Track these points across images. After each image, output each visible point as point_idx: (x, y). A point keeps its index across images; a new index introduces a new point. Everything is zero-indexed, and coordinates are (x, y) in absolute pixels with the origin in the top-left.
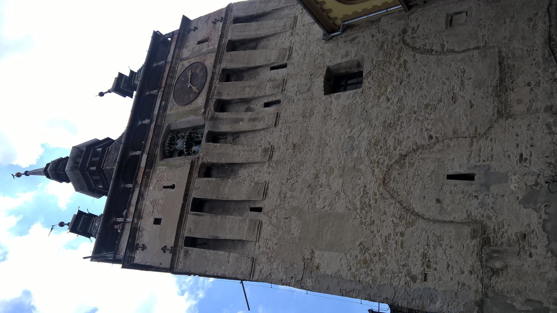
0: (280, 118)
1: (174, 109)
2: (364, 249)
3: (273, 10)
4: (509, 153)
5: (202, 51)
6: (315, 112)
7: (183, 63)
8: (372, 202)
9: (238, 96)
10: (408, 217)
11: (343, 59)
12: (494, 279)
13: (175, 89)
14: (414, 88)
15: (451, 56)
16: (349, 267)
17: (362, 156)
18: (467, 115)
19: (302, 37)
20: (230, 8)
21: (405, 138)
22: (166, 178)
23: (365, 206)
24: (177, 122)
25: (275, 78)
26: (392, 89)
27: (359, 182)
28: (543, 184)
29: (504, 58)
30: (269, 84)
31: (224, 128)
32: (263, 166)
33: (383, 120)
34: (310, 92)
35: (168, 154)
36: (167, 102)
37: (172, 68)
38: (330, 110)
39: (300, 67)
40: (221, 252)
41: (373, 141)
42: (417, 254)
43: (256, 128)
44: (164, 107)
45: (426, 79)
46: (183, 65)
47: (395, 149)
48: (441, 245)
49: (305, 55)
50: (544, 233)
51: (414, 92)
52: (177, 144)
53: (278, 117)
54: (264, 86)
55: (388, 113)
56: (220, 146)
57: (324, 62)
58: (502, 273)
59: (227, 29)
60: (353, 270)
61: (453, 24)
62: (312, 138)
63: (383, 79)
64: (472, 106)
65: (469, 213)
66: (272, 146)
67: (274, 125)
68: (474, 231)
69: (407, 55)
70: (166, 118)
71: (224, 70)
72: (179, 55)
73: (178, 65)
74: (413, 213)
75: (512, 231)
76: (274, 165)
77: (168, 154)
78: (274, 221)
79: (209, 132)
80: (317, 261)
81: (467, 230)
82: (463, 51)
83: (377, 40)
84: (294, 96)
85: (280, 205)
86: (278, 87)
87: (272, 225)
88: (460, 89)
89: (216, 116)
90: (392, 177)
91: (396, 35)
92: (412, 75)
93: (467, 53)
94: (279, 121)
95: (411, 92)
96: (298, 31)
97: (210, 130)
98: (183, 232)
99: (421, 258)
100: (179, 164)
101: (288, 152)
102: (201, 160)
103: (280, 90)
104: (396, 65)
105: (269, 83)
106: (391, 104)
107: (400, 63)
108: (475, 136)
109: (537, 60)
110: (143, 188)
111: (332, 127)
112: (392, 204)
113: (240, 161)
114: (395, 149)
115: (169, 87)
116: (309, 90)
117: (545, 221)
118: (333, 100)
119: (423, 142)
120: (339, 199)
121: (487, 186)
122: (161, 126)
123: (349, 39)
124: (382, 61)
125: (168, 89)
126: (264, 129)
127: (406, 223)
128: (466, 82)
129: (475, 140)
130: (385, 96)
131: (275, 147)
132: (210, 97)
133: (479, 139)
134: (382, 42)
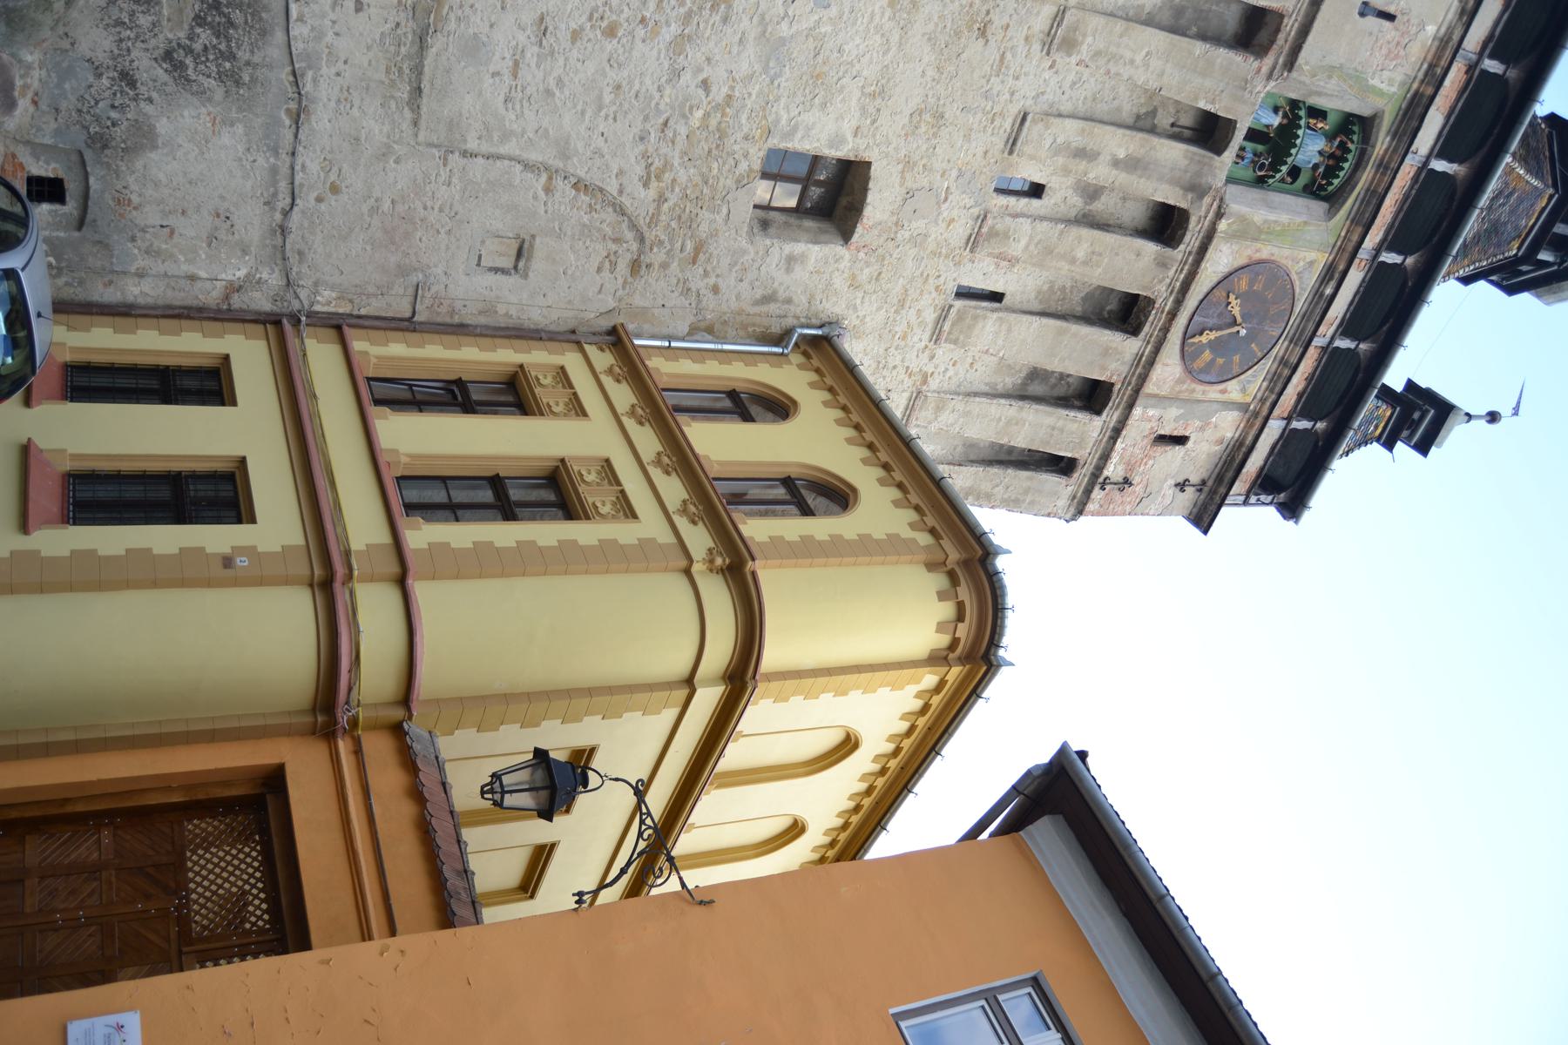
0: (1007, 134)
1: (1302, 264)
3: (960, 465)
5: (1182, 411)
6: (906, 120)
7: (1241, 395)
9: (1113, 240)
11: (803, 252)
13: (1284, 325)
14: (637, 96)
15: (533, 156)
19: (899, 358)
22: (1379, 44)
24: (1303, 218)
25: (997, 266)
30: (1016, 249)
31: (1175, 154)
34: (909, 184)
35: (1356, 128)
36: (1317, 293)
37: (1277, 389)
38: (863, 109)
39: (922, 275)
43: (1081, 126)
44: (1331, 279)
45: (603, 113)
46: (1244, 390)
49: (902, 303)
51: (637, 87)
52: (1320, 153)
53: (1011, 141)
54: (1032, 247)
55: (712, 44)
56: (1196, 99)
57: (854, 261)
59: (1096, 450)
61: (515, 246)
62: (929, 39)
63: (710, 152)
66: (1048, 53)
67: (1029, 118)
69: (640, 199)
70: (1332, 241)
71: (1134, 331)
72: (1249, 424)
77: (1356, 128)
79: (1219, 152)
82: (499, 157)
83: (706, 274)
84: (953, 189)
86: (993, 234)
88: (523, 51)
89: (1190, 196)
91: (656, 268)
92: (634, 138)
93: (493, 150)
95: (644, 90)
96: (908, 382)
97: (1216, 157)
100: (1330, 77)
101: (1006, 20)
102: (1265, 70)
103: (990, 222)
104: (670, 181)
105: (1014, 253)
109: (333, 71)
110: (1456, 37)
111: (868, 56)
113: (1150, 32)
115: (1301, 334)
116: (910, 194)
118: (850, 138)
122: (1352, 221)
123: (779, 305)
124: (704, 208)
126: (1060, 115)
130: (713, 100)
131: (1039, 48)
132: (1191, 258)
134: (694, 262)
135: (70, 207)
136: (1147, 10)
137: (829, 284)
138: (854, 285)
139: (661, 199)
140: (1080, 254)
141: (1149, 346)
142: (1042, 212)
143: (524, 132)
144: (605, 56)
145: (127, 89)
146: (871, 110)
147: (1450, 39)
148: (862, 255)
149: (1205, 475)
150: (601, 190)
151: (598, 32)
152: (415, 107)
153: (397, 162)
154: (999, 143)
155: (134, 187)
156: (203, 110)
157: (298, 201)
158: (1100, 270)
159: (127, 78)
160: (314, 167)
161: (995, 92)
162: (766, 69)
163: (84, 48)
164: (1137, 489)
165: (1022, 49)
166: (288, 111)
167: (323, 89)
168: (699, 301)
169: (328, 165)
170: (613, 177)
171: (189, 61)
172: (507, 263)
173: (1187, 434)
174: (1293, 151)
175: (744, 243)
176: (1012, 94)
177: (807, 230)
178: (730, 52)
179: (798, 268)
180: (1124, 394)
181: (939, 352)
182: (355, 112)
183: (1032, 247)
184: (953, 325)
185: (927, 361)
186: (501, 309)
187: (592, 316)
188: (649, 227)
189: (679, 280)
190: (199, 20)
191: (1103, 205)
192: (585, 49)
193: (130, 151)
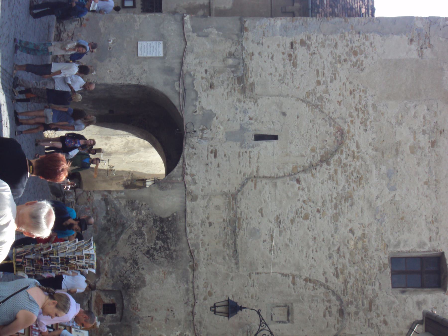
4: (225, 159)
8: (355, 114)
10: (314, 99)
12: (233, 49)
14: (323, 240)
15: (286, 272)
16: (373, 45)
18: (265, 201)
21: (326, 183)
23: (363, 109)
26: (348, 243)
27: (374, 136)
28: (198, 130)
29: (233, 257)
33: (355, 207)
38: (430, 230)
41: (363, 182)
45: (311, 249)
47: (336, 171)
48: (280, 75)
50: (197, 90)
51: (322, 237)
58: (227, 55)
60: (367, 43)
61: (286, 309)
63: (362, 258)
64: (261, 211)
65: (256, 104)
68: (252, 90)
74: (308, 104)
75: (220, 90)
80: (414, 47)
81: (258, 90)
83: (378, 315)
88: (273, 231)
91: (353, 314)
99: (298, 63)
106: (347, 226)
107: (344, 276)
109: (204, 249)
112: (333, 113)
114: (336, 171)
120: (398, 117)
121: (242, 129)
124: (368, 284)
127: (315, 94)
128: (267, 238)
129: (255, 174)
134: (370, 310)
139: (346, 282)
143: (280, 262)
144: (306, 227)
145: (135, 266)
146: (434, 228)
150: (317, 281)
151: (301, 219)
155: (138, 302)
156: (161, 270)
157: (197, 301)
159: (135, 262)
160: (201, 286)
166: (190, 266)
168: (379, 330)
170: (322, 275)
171: (155, 253)
172: (285, 319)
175: (392, 298)
177: (425, 291)
178: (358, 216)
188: (344, 295)
189: (365, 319)
190: (158, 238)
192: (297, 226)
193: (138, 288)
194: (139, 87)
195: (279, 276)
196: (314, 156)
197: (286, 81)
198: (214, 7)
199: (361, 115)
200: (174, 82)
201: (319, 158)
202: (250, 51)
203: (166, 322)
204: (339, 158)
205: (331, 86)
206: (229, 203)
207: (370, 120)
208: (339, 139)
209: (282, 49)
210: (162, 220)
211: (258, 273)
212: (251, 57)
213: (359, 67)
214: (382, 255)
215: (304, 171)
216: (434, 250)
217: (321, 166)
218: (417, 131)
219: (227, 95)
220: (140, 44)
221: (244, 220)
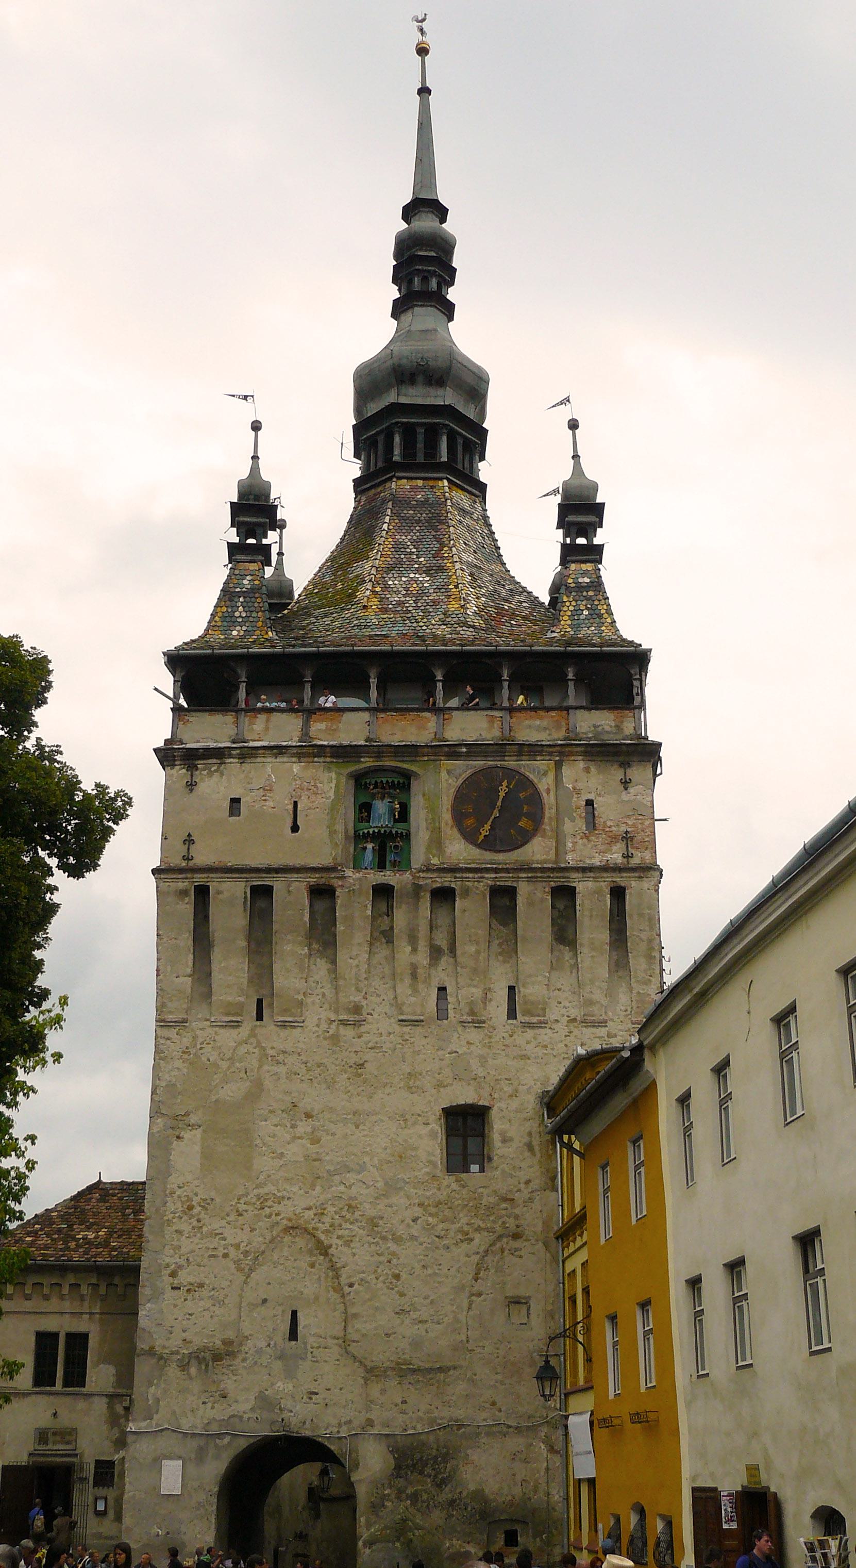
2: (205, 1204)
4: (320, 1381)
5: (566, 819)
6: (415, 1095)
8: (267, 1211)
10: (247, 1262)
17: (334, 1189)
20: (651, 870)
23: (261, 1200)
31: (400, 917)
32: (330, 1009)
37: (539, 749)
38: (415, 1124)
40: (191, 956)
41: (353, 1204)
42: (202, 1275)
44: (455, 752)
46: (545, 774)
47: (339, 1237)
51: (422, 1257)
53: (416, 1023)
55: (394, 1222)
56: (367, 917)
60: (179, 1192)
63: (449, 1208)
66: (365, 1021)
68: (231, 1343)
69: (480, 1241)
72: (571, 754)
73: (547, 758)
74: (251, 1270)
75: (229, 1384)
76: (331, 1032)
78: (243, 1050)
80: (187, 1135)
81: (231, 1334)
83: (519, 1190)
84: (449, 1050)
85: (266, 1055)
86: (472, 1013)
87: (236, 1047)
89: (422, 894)
90: (297, 1239)
94: (406, 1026)
96: (576, 1032)
98: (216, 880)
102: (340, 883)
108: (345, 1342)
110: (295, 751)
114: (339, 1237)
117: (241, 1418)
119: (344, 1276)
125: (492, 752)
127: (239, 1260)
129: (340, 1341)
133: (340, 1346)
135: (517, 1527)
136: (329, 966)
137: (517, 1111)
138: (515, 1094)
139: (478, 1229)
140: (472, 949)
141: (521, 875)
142: (454, 983)
143: (453, 1311)
145: (457, 1503)
147: (297, 753)
148: (496, 1096)
149: (616, 766)
150: (477, 1264)
152: (449, 1369)
153: (475, 1375)
154: (419, 1030)
156: (462, 1469)
158: (480, 932)
159: (452, 1503)
161: (391, 1045)
162: (401, 1189)
163: (441, 1522)
164: (630, 823)
165: (365, 1038)
167: (445, 1414)
168: (536, 1190)
169: (481, 1408)
172: (525, 1307)
173: (584, 803)
174: (382, 832)
176: (390, 1033)
179: (509, 1134)
180: (557, 877)
181: (553, 1017)
182: (454, 1398)
183: (475, 983)
184: (533, 1015)
185: (559, 1024)
186: (549, 1307)
187: (548, 1255)
188: (495, 1232)
190: (421, 1473)
191: (441, 940)
193: (486, 1501)
194: (220, 1495)
195: (471, 1313)
196: (320, 1264)
197: (221, 1297)
198: (112, 1390)
199: (269, 1203)
200: (216, 1445)
201: (322, 1258)
202: (180, 1342)
203: (528, 1462)
204: (322, 1233)
205: (230, 1240)
206: (376, 1376)
207: (276, 1192)
208: (299, 1231)
209: (179, 1302)
210: (398, 1467)
211: (468, 1341)
212: (188, 1342)
213: (208, 1204)
214: (445, 1183)
215: (338, 1277)
216: (440, 1119)
217: (333, 1255)
218: (293, 1135)
219: (236, 1375)
220: (164, 1491)
221: (399, 1358)
